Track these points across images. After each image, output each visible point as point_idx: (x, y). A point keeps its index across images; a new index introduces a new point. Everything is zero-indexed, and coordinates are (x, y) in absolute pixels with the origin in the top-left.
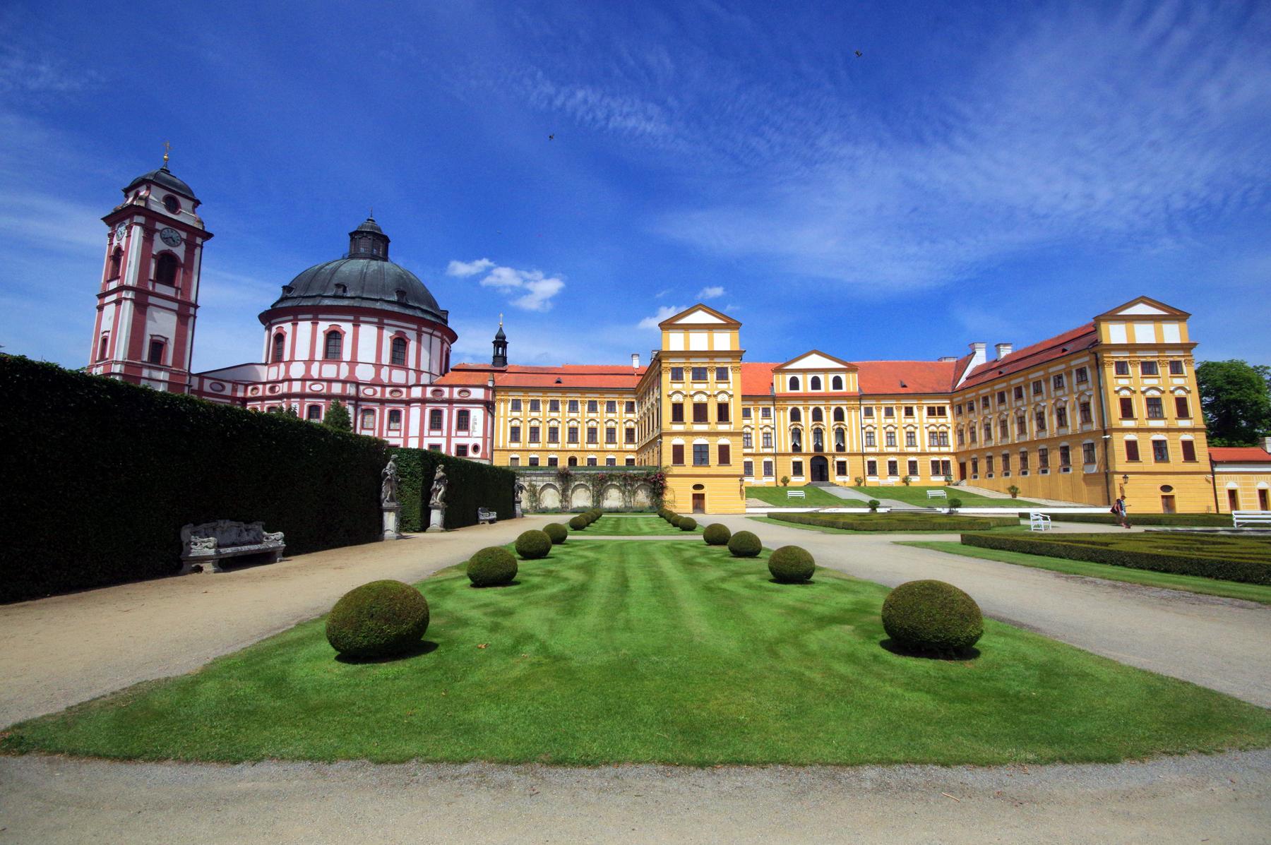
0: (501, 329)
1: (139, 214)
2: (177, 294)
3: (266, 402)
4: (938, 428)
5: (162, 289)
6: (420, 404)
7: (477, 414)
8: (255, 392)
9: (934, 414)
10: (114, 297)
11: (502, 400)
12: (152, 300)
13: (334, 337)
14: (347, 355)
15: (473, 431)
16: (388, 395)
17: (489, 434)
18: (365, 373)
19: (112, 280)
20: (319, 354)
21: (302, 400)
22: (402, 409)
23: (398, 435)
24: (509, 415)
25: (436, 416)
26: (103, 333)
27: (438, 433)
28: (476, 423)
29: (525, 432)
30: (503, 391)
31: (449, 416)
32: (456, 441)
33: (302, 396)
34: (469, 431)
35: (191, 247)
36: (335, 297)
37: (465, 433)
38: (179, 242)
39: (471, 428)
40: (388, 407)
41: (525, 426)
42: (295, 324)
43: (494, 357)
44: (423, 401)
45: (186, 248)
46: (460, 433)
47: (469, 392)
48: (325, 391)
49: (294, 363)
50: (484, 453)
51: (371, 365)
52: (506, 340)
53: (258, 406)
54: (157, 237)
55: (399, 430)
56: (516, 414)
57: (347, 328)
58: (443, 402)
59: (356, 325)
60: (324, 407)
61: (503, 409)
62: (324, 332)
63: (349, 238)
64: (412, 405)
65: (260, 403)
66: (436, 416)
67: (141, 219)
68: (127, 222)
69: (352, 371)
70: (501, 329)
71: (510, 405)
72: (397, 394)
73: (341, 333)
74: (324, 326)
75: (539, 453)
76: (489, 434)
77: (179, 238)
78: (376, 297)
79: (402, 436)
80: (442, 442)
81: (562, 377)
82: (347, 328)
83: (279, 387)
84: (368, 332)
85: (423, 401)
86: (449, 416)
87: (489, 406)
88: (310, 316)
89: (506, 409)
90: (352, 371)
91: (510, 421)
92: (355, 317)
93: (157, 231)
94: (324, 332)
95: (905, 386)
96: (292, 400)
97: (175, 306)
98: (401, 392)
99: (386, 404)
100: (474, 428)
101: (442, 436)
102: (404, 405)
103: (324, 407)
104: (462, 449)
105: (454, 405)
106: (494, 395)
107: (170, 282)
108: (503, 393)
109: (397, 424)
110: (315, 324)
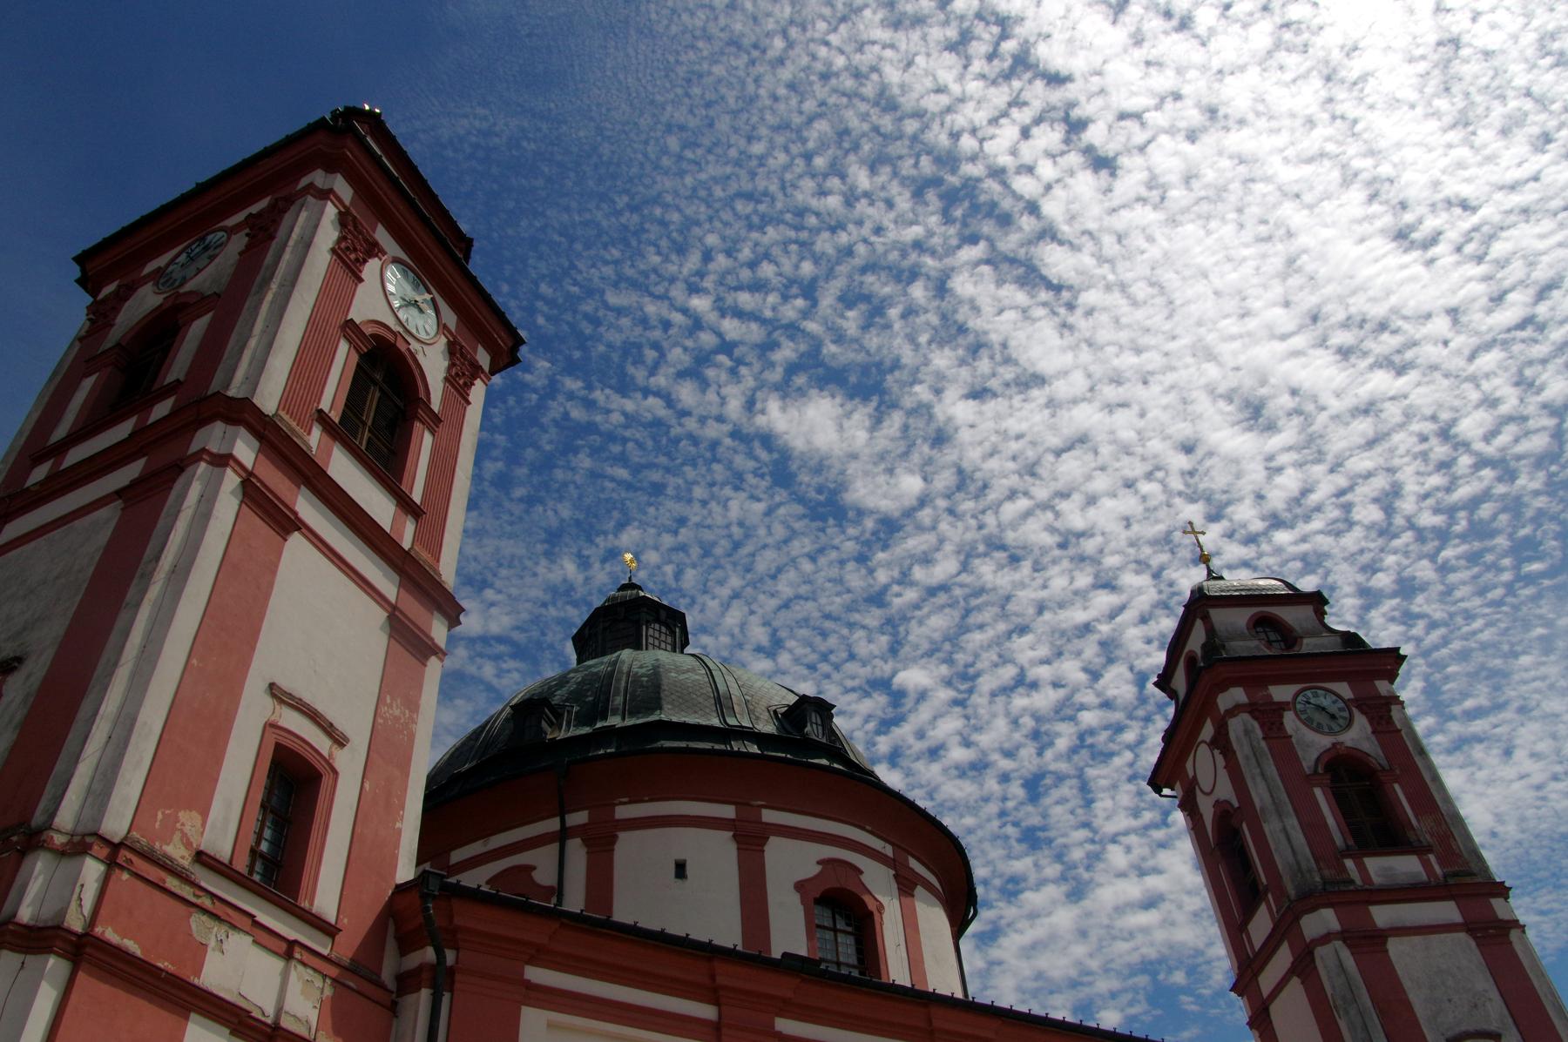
1: (1224, 686)
2: (1426, 865)
5: (1383, 868)
10: (1283, 958)
12: (1382, 915)
19: (1248, 912)
35: (1383, 712)
38: (1346, 714)
45: (1371, 721)
54: (1290, 721)
67: (1237, 695)
68: (1208, 731)
77: (1341, 704)
93: (1282, 707)
97: (1447, 911)
107: (1393, 839)
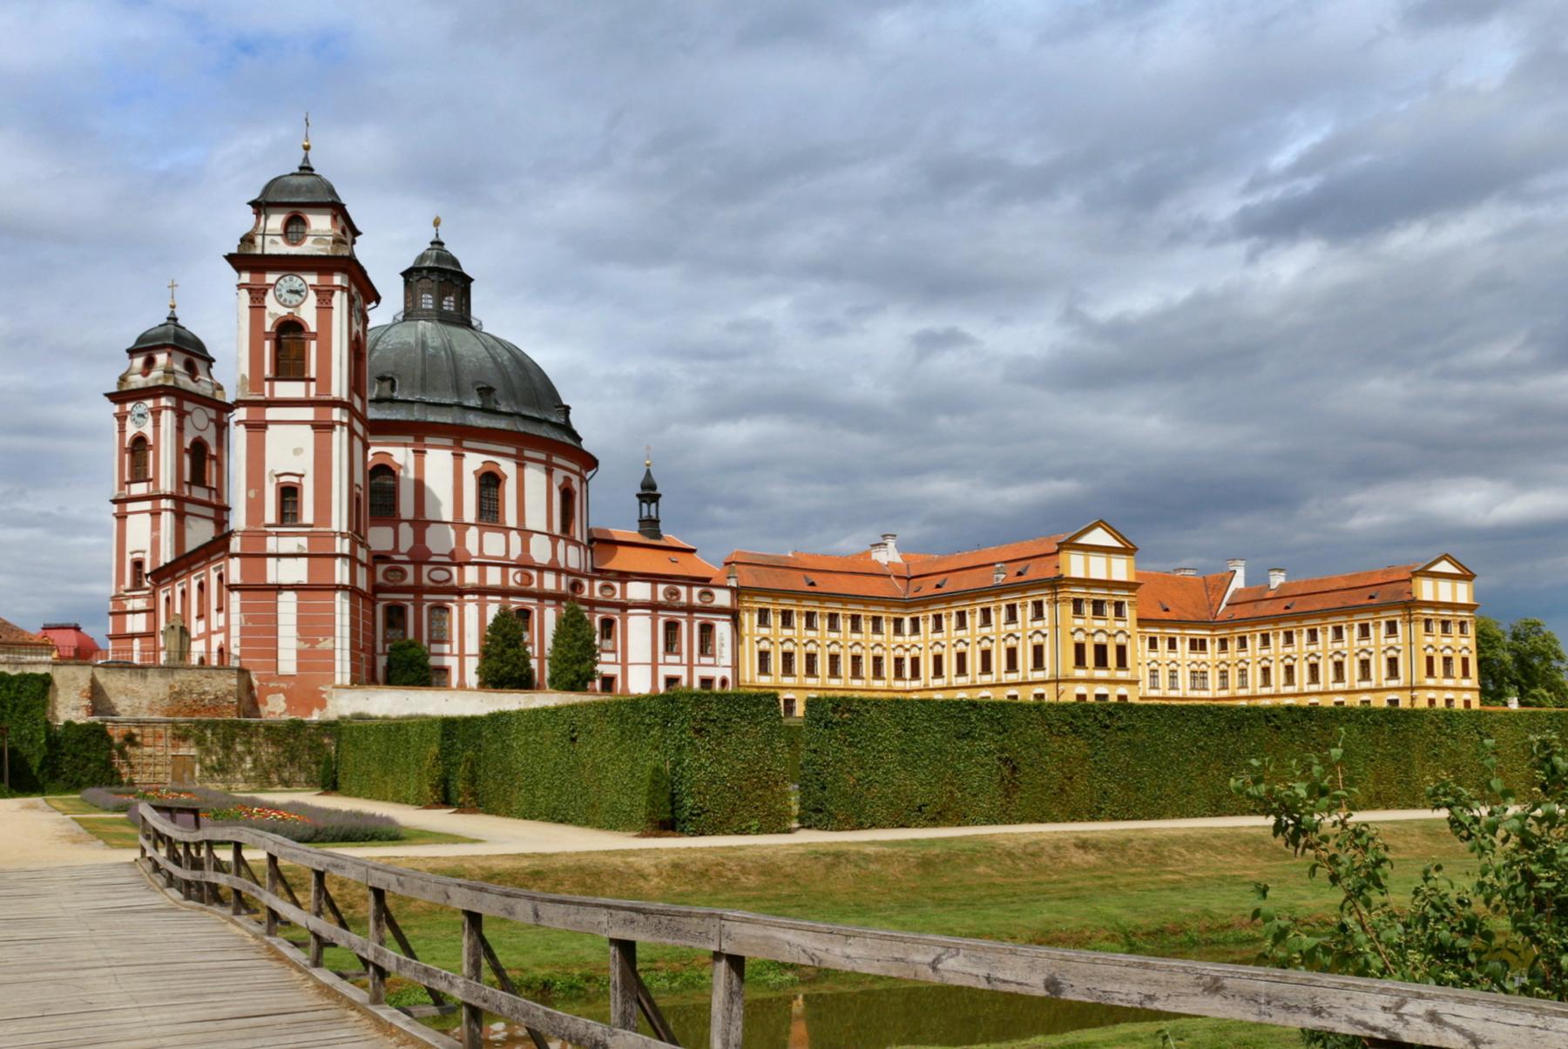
0: (648, 471)
3: (426, 597)
4: (1199, 666)
6: (649, 612)
7: (723, 628)
8: (391, 575)
9: (1196, 649)
11: (749, 610)
13: (490, 481)
14: (511, 519)
15: (721, 657)
16: (597, 594)
17: (736, 666)
18: (541, 551)
20: (470, 514)
21: (505, 599)
22: (616, 617)
23: (614, 660)
24: (756, 632)
25: (672, 627)
26: (278, 476)
27: (675, 659)
28: (722, 645)
29: (776, 658)
30: (747, 594)
31: (689, 631)
32: (700, 672)
33: (504, 592)
34: (713, 655)
36: (484, 410)
37: (709, 660)
39: (717, 653)
40: (599, 612)
41: (776, 649)
42: (419, 453)
43: (640, 521)
44: (653, 607)
46: (705, 660)
47: (711, 595)
48: (535, 585)
49: (432, 525)
50: (733, 688)
51: (547, 537)
52: (658, 491)
53: (408, 603)
55: (614, 651)
56: (764, 631)
57: (507, 467)
58: (681, 609)
59: (521, 466)
60: (536, 612)
61: (749, 620)
62: (475, 472)
63: (402, 279)
64: (630, 611)
65: (411, 596)
66: (672, 627)
69: (525, 547)
70: (648, 472)
71: (756, 617)
72: (608, 592)
73: (501, 477)
74: (474, 462)
75: (795, 691)
76: (736, 666)
78: (536, 415)
79: (619, 661)
80: (681, 672)
81: (813, 577)
82: (507, 467)
83: (516, 582)
84: (535, 477)
85: (653, 607)
86: (689, 631)
87: (734, 616)
88: (449, 442)
89: (751, 622)
90: (525, 547)
91: (758, 642)
92: (517, 449)
94: (475, 472)
95: (1167, 610)
96: (489, 598)
98: (612, 588)
99: (597, 609)
100: (721, 652)
101: (680, 664)
102: (618, 611)
103: (536, 612)
104: (707, 682)
105: (696, 615)
106: (738, 601)
108: (746, 598)
109: (609, 641)
110: (458, 457)
